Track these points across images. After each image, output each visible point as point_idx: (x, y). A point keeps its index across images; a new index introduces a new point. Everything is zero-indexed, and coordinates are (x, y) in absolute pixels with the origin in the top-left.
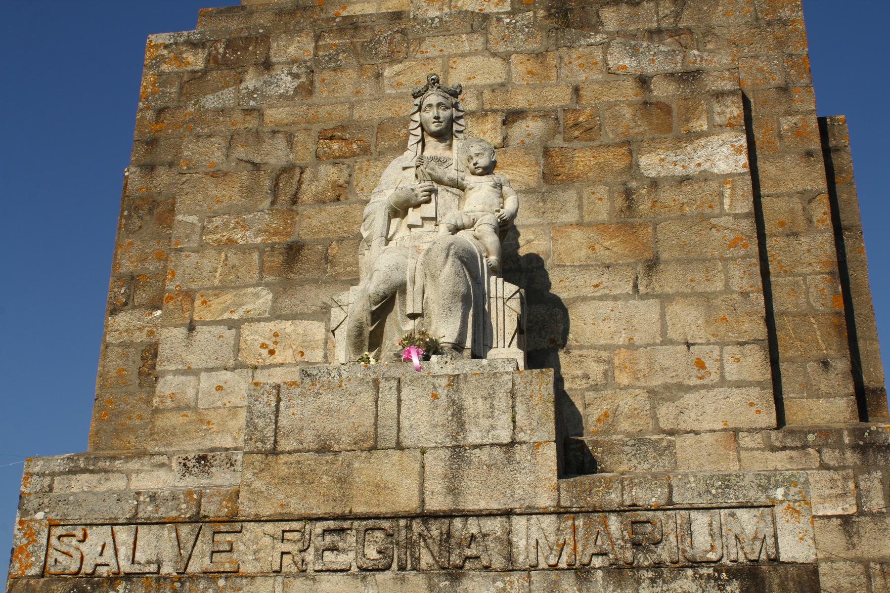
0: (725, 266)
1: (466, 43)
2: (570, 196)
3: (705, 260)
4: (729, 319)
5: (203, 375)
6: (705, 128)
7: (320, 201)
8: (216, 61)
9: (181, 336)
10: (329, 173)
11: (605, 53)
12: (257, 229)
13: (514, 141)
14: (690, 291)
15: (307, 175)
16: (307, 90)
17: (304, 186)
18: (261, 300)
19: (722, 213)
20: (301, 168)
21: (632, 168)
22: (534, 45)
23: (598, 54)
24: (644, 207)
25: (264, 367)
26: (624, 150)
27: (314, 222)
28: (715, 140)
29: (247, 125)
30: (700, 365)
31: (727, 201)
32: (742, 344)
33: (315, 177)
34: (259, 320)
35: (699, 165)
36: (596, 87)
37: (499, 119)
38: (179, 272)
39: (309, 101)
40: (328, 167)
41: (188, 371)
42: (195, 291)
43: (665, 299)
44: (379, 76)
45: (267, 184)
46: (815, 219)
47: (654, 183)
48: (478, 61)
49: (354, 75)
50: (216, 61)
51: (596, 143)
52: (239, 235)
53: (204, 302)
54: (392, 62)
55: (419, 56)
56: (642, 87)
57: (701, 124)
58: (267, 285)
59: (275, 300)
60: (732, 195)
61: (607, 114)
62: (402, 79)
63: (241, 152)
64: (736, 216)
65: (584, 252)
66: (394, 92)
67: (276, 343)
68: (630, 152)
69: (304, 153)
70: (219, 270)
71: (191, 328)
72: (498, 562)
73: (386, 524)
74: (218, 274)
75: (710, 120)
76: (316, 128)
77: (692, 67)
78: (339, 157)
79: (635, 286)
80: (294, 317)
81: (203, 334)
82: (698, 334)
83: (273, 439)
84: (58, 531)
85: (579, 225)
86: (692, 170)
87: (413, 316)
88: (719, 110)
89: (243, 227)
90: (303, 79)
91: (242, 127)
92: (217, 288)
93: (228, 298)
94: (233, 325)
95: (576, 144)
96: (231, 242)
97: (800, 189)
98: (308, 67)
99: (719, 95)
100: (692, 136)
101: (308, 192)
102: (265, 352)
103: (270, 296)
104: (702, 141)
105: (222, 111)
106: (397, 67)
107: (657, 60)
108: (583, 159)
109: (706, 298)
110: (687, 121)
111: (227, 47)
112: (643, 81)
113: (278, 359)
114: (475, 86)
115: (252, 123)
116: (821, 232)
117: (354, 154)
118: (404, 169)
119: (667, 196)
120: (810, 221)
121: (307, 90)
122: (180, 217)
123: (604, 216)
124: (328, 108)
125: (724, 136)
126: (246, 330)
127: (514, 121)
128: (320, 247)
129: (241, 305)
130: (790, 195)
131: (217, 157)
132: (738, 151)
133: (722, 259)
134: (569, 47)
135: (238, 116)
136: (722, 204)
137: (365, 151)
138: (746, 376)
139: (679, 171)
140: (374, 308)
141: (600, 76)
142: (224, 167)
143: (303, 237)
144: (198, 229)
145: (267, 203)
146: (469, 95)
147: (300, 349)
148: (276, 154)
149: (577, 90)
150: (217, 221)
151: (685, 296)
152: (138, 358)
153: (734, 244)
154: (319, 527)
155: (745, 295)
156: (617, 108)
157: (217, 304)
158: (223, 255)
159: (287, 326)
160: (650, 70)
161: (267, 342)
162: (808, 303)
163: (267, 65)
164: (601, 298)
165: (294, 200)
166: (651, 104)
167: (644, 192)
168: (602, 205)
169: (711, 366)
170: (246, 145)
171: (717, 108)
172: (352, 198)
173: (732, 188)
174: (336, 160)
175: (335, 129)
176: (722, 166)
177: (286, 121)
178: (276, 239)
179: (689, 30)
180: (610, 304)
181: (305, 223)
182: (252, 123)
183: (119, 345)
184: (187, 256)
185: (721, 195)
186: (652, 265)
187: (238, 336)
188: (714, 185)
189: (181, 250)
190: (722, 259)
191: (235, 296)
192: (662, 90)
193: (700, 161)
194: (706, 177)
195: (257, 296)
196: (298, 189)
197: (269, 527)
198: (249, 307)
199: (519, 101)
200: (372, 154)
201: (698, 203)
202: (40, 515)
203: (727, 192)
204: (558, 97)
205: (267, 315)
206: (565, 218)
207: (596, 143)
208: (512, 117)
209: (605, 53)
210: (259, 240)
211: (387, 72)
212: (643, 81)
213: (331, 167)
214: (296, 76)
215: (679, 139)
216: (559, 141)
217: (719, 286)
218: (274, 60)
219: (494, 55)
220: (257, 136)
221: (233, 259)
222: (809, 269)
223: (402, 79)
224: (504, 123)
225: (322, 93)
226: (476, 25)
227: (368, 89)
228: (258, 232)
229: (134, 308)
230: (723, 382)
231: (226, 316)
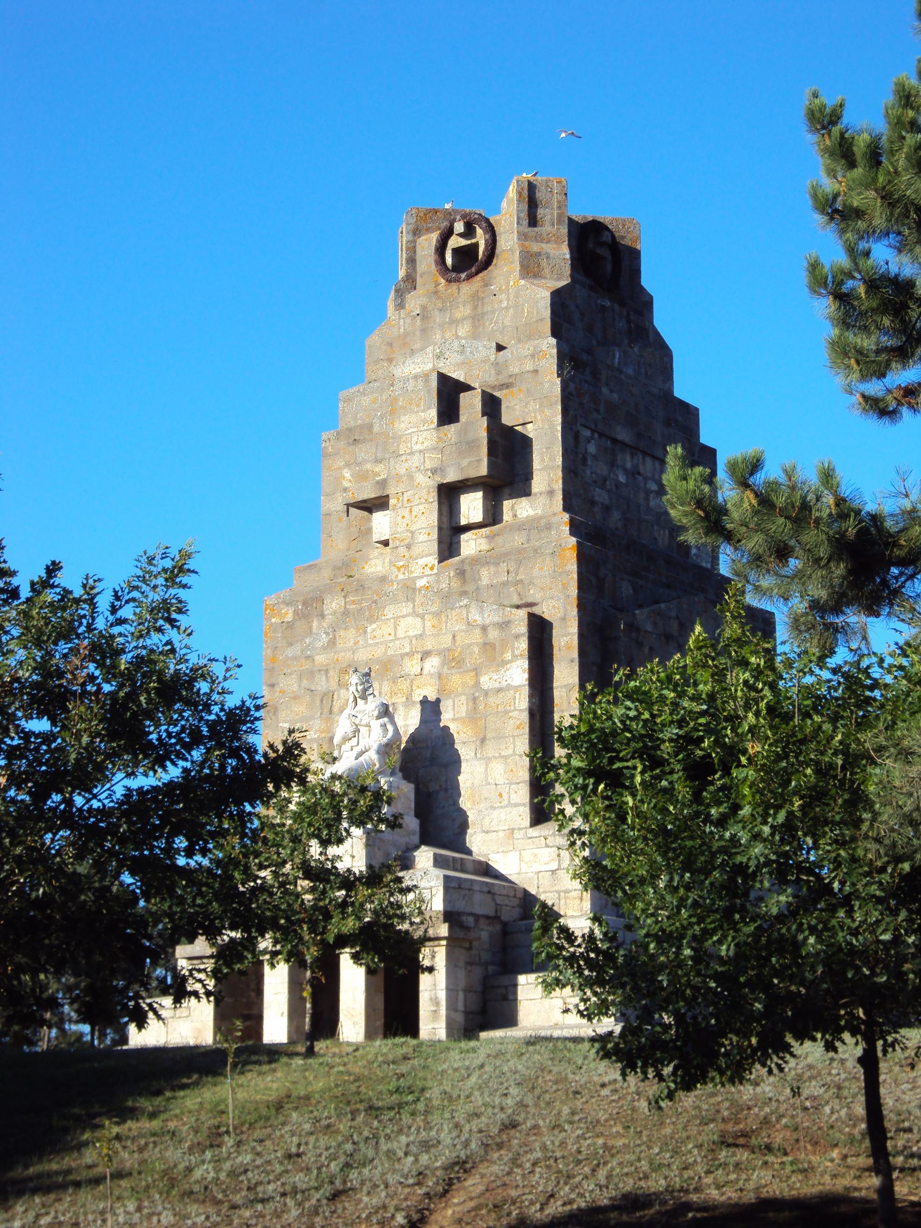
16: (332, 643)
19: (515, 709)
21: (477, 684)
22: (434, 608)
28: (514, 664)
30: (500, 795)
43: (488, 760)
44: (365, 632)
47: (486, 693)
48: (410, 619)
54: (372, 623)
57: (508, 656)
62: (377, 633)
63: (305, 683)
75: (513, 652)
82: (501, 780)
86: (504, 684)
95: (453, 671)
100: (504, 663)
105: (295, 658)
106: (374, 626)
112: (484, 629)
119: (492, 700)
121: (332, 643)
131: (295, 688)
132: (524, 671)
138: (519, 801)
139: (497, 685)
148: (321, 684)
163: (322, 616)
169: (505, 796)
179: (521, 581)
186: (483, 741)
188: (512, 692)
192: (493, 634)
194: (509, 687)
199: (429, 645)
204: (446, 641)
208: (426, 655)
211: (369, 630)
212: (484, 629)
214: (327, 634)
215: (498, 666)
219: (417, 616)
220: (311, 674)
225: (340, 645)
227: (361, 639)
230: (510, 804)
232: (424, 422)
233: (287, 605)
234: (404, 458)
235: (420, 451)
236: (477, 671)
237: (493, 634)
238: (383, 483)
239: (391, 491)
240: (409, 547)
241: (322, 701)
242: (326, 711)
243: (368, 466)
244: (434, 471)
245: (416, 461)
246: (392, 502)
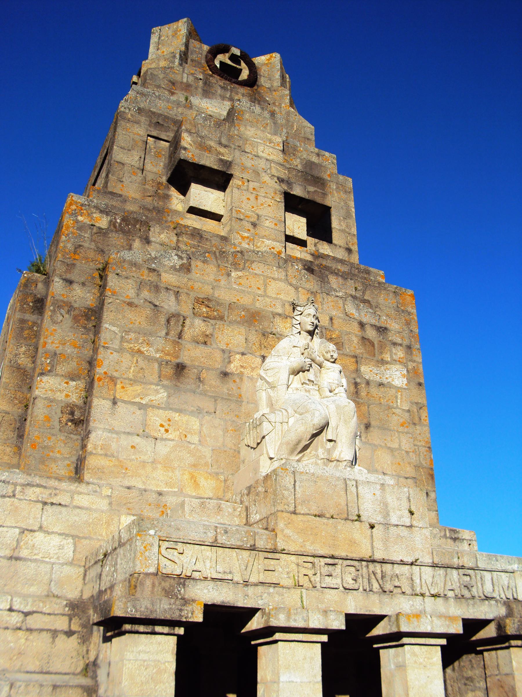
0: (399, 435)
4: (401, 464)
5: (123, 436)
8: (115, 227)
9: (107, 406)
12: (157, 348)
14: (384, 445)
15: (188, 322)
16: (186, 269)
18: (160, 395)
19: (397, 407)
20: (184, 317)
21: (357, 370)
23: (341, 302)
24: (363, 394)
25: (162, 439)
27: (191, 354)
29: (150, 279)
31: (399, 401)
32: (406, 478)
33: (192, 325)
34: (159, 408)
35: (387, 378)
36: (341, 321)
38: (106, 363)
39: (189, 276)
40: (200, 321)
41: (112, 431)
42: (118, 378)
44: (229, 275)
45: (163, 320)
46: (422, 418)
49: (215, 269)
50: (115, 227)
52: (145, 349)
53: (123, 387)
54: (236, 269)
55: (251, 270)
56: (361, 328)
58: (164, 386)
59: (169, 397)
60: (401, 399)
61: (346, 337)
62: (243, 281)
66: (237, 288)
67: (169, 425)
68: (357, 362)
69: (186, 309)
70: (133, 368)
71: (114, 403)
72: (408, 591)
73: (356, 563)
74: (131, 371)
76: (193, 295)
78: (206, 317)
80: (180, 411)
81: (121, 408)
83: (294, 504)
84: (165, 545)
87: (330, 441)
89: (147, 344)
90: (185, 261)
91: (147, 279)
92: (131, 380)
93: (138, 388)
94: (141, 407)
96: (139, 352)
97: (416, 401)
98: (188, 255)
100: (383, 362)
101: (188, 334)
102: (162, 429)
103: (166, 394)
104: (388, 366)
106: (240, 274)
109: (391, 450)
110: (381, 353)
111: (123, 220)
112: (362, 325)
113: (170, 436)
114: (281, 299)
116: (426, 426)
117: (215, 318)
118: (294, 347)
122: (107, 326)
128: (196, 371)
129: (147, 395)
131: (132, 293)
133: (397, 431)
136: (397, 402)
137: (222, 318)
139: (377, 379)
140: (315, 432)
141: (342, 315)
142: (136, 301)
143: (186, 362)
144: (118, 337)
145: (164, 333)
146: (277, 303)
147: (184, 433)
148: (169, 304)
149: (331, 319)
150: (132, 335)
152: (59, 411)
154: (323, 561)
155: (407, 452)
156: (350, 336)
157: (130, 389)
158: (135, 359)
159: (176, 416)
160: (364, 320)
161: (164, 424)
162: (420, 461)
165: (180, 336)
166: (365, 339)
167: (363, 386)
170: (150, 291)
171: (394, 351)
172: (214, 346)
173: (401, 395)
174: (206, 318)
177: (174, 284)
178: (168, 358)
181: (186, 353)
183: (45, 399)
184: (112, 353)
185: (396, 397)
187: (146, 414)
189: (107, 348)
191: (143, 388)
192: (371, 333)
193: (387, 376)
194: (390, 386)
195: (157, 392)
197: (293, 558)
198: (153, 398)
200: (225, 321)
201: (387, 399)
202: (152, 532)
203: (399, 396)
205: (163, 406)
210: (158, 355)
211: (233, 274)
212: (362, 325)
213: (202, 322)
214: (180, 258)
218: (152, 239)
221: (142, 363)
223: (243, 281)
225: (196, 274)
226: (281, 264)
228: (157, 351)
229: (57, 375)
231: (137, 400)
232: (271, 142)
233: (101, 212)
237: (371, 333)
240: (254, 225)
241: (168, 321)
242: (173, 333)
243: (212, 144)
244: (281, 180)
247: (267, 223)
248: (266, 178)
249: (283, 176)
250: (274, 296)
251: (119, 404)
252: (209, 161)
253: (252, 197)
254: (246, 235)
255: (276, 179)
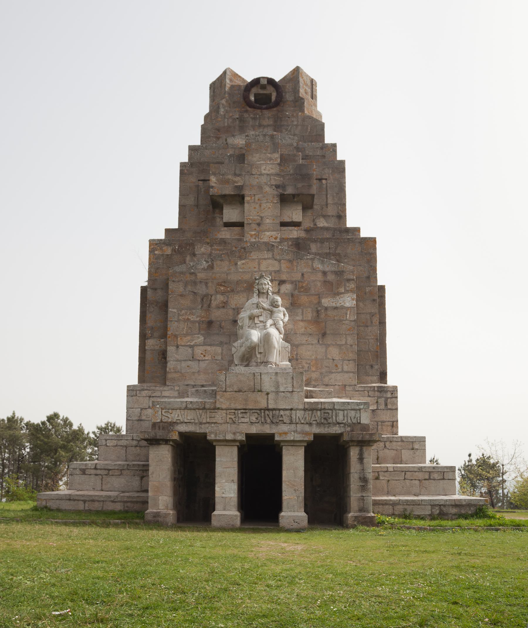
1: (266, 255)
2: (300, 311)
3: (340, 334)
6: (343, 291)
7: (218, 307)
10: (220, 298)
11: (312, 263)
13: (282, 291)
15: (213, 298)
16: (211, 267)
17: (212, 302)
21: (319, 303)
23: (310, 262)
24: (322, 316)
26: (317, 297)
27: (216, 314)
31: (348, 316)
33: (216, 299)
34: (200, 346)
36: (309, 274)
37: (277, 283)
43: (327, 346)
45: (199, 300)
47: (326, 309)
51: (308, 294)
58: (201, 334)
59: (205, 339)
60: (350, 314)
63: (189, 288)
64: (351, 321)
65: (303, 329)
68: (319, 297)
69: (211, 291)
71: (177, 347)
77: (340, 270)
79: (319, 341)
81: (181, 349)
85: (302, 321)
88: (348, 285)
90: (210, 263)
93: (189, 338)
96: (188, 319)
97: (370, 312)
99: (348, 280)
100: (339, 294)
101: (214, 304)
104: (342, 296)
107: (330, 266)
108: (304, 299)
110: (338, 288)
112: (324, 273)
113: (206, 358)
114: (269, 270)
115: (193, 278)
117: (229, 292)
119: (330, 313)
120: (372, 322)
122: (170, 310)
123: (310, 318)
124: (219, 274)
125: (349, 294)
126: (196, 349)
127: (282, 284)
130: (367, 314)
131: (181, 289)
133: (345, 334)
134: (301, 259)
135: (188, 275)
139: (334, 305)
142: (184, 293)
144: (177, 314)
145: (200, 307)
148: (202, 290)
149: (303, 275)
150: (183, 312)
151: (333, 345)
153: (349, 330)
155: (351, 346)
159: (208, 348)
160: (327, 269)
164: (308, 344)
165: (209, 306)
168: (309, 315)
172: (228, 307)
174: (223, 293)
175: (222, 282)
176: (348, 305)
178: (204, 319)
180: (311, 346)
182: (193, 278)
185: (346, 314)
186: (324, 335)
187: (193, 350)
189: (172, 321)
190: (345, 334)
192: (331, 277)
194: (342, 307)
195: (198, 338)
196: (210, 303)
199: (284, 277)
203: (348, 313)
204: (297, 276)
206: (298, 318)
207: (308, 294)
209: (312, 263)
212: (324, 273)
214: (207, 262)
216: (296, 292)
217: (344, 343)
220: (195, 283)
222: (370, 338)
224: (279, 284)
225: (216, 269)
226: (270, 248)
227: (233, 269)
228: (197, 317)
231: (189, 343)
234: (256, 176)
235: (268, 175)
236: (319, 296)
238: (241, 188)
239: (246, 192)
240: (259, 224)
241: (202, 299)
242: (205, 306)
243: (230, 177)
244: (277, 187)
245: (264, 179)
246: (247, 199)
247: (268, 221)
248: (267, 189)
249: (278, 183)
250: (265, 270)
251: (180, 347)
252: (228, 190)
253: (257, 206)
254: (253, 233)
255: (274, 187)
